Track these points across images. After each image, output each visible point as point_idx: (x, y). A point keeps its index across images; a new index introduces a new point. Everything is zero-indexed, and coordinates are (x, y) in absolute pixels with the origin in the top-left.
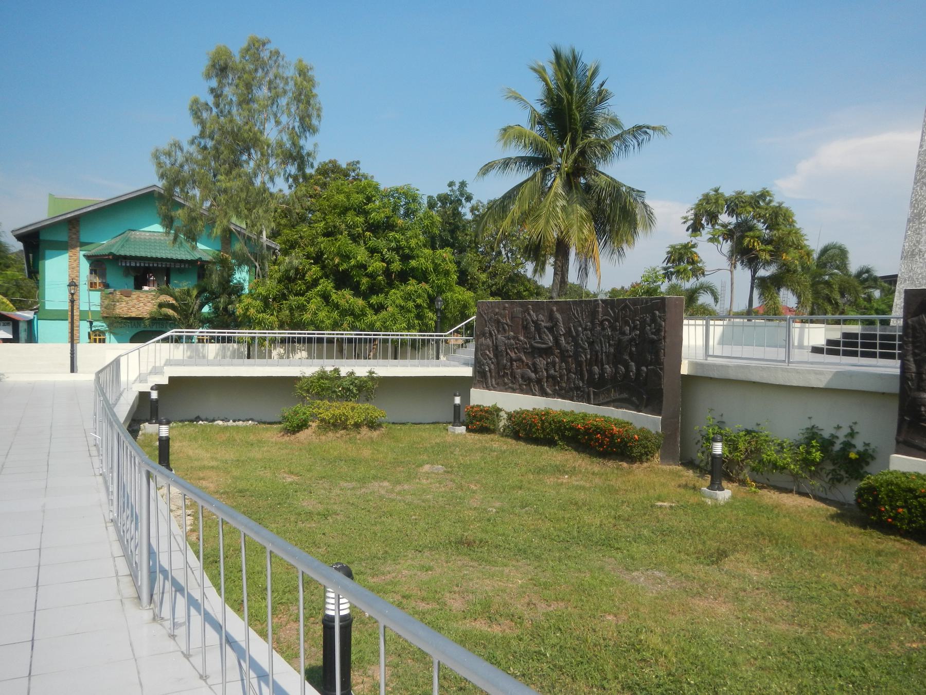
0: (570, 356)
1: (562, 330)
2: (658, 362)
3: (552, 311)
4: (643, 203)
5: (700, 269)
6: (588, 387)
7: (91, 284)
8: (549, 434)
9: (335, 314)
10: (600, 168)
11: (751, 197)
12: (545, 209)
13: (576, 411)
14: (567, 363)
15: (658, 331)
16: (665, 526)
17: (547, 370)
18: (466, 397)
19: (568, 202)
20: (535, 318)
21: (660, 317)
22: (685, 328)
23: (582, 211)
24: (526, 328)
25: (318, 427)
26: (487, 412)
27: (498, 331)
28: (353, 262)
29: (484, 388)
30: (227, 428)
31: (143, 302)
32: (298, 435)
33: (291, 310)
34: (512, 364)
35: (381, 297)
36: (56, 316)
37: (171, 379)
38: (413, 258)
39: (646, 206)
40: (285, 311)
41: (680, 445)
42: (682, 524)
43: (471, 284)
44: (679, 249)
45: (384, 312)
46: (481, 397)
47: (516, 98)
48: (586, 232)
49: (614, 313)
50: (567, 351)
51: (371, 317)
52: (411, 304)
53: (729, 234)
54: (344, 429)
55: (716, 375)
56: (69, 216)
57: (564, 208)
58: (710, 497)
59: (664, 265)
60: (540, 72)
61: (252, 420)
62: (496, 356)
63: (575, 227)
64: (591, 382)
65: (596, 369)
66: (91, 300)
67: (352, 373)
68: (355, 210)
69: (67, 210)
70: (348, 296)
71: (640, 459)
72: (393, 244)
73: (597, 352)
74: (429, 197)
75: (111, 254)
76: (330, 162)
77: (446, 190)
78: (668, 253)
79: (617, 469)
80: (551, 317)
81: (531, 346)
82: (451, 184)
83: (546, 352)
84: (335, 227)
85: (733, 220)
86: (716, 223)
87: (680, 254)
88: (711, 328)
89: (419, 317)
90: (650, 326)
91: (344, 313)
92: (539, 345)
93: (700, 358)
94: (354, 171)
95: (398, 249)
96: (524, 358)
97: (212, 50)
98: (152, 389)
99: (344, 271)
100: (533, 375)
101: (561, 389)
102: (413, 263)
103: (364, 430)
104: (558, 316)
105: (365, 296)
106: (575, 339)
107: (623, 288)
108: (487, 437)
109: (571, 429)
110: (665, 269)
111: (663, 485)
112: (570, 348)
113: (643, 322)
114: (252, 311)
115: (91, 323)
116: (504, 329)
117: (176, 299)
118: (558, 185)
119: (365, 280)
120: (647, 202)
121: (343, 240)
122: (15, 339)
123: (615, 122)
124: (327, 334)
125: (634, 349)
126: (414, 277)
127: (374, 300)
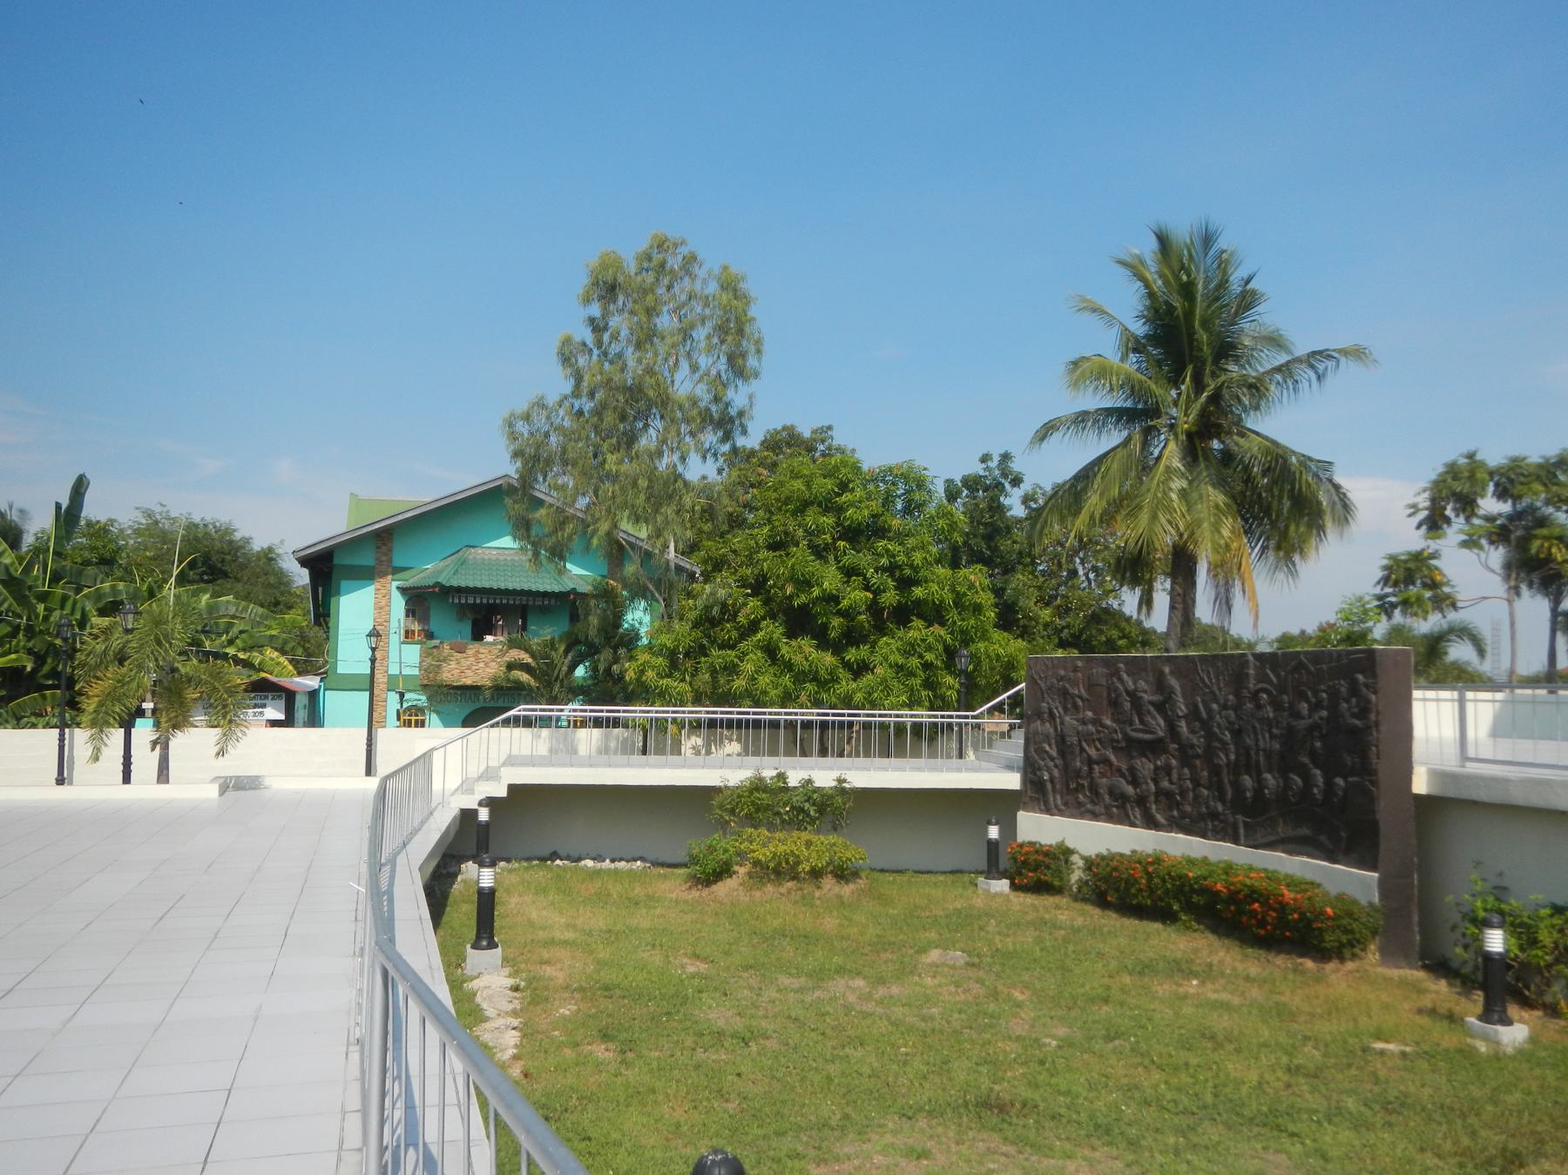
0: (1198, 756)
1: (1182, 709)
2: (1366, 770)
3: (1162, 673)
4: (1330, 481)
5: (1448, 596)
6: (1234, 814)
7: (407, 632)
8: (1161, 899)
9: (787, 680)
10: (1250, 423)
11: (1540, 466)
12: (1150, 496)
13: (1213, 858)
14: (1192, 767)
15: (1364, 710)
16: (1392, 1094)
17: (1155, 781)
18: (1009, 828)
19: (1190, 482)
20: (1131, 686)
21: (1367, 686)
22: (1418, 709)
23: (1218, 497)
24: (1114, 704)
25: (749, 874)
26: (1047, 854)
27: (1066, 709)
28: (816, 592)
29: (1041, 811)
30: (598, 872)
31: (483, 662)
32: (714, 888)
33: (714, 672)
34: (1091, 769)
35: (864, 650)
36: (349, 684)
37: (511, 788)
38: (917, 583)
39: (1337, 487)
40: (703, 675)
41: (1420, 931)
42: (1427, 1091)
43: (1025, 627)
44: (1406, 562)
45: (870, 677)
46: (1038, 828)
47: (1094, 310)
48: (1226, 533)
49: (1278, 676)
50: (1192, 746)
51: (846, 684)
52: (914, 662)
53: (1500, 533)
54: (793, 879)
55: (1482, 795)
56: (377, 526)
57: (1183, 494)
58: (1485, 1038)
59: (1378, 590)
60: (1135, 269)
61: (642, 859)
62: (1062, 753)
63: (1205, 525)
64: (1239, 804)
65: (1247, 781)
66: (406, 658)
67: (810, 781)
68: (820, 505)
69: (376, 517)
70: (808, 649)
71: (1337, 953)
72: (884, 561)
73: (1247, 749)
74: (947, 481)
75: (437, 584)
76: (785, 428)
77: (978, 469)
78: (1386, 568)
79: (1295, 971)
80: (1160, 685)
81: (1125, 735)
82: (985, 459)
83: (1153, 748)
84: (786, 533)
85: (1505, 507)
86: (1473, 514)
87: (1408, 569)
88: (1470, 707)
89: (929, 684)
90: (1347, 701)
91: (801, 677)
92: (1141, 735)
93: (1451, 763)
94: (823, 441)
95: (891, 569)
96: (1113, 758)
97: (594, 261)
98: (480, 804)
99: (804, 608)
100: (1130, 790)
101: (1183, 815)
102: (918, 592)
103: (828, 882)
104: (1174, 683)
105: (837, 648)
106: (1206, 725)
107: (1303, 632)
108: (1050, 900)
109: (1204, 891)
110: (1380, 598)
111: (1386, 1007)
112: (1198, 741)
113: (1334, 695)
114: (650, 674)
115: (402, 695)
116: (1075, 706)
117: (533, 656)
118: (1170, 453)
119: (836, 622)
120: (1338, 479)
121: (800, 553)
122: (288, 722)
123: (1275, 341)
124: (769, 713)
125: (1318, 744)
126: (920, 616)
127: (852, 655)
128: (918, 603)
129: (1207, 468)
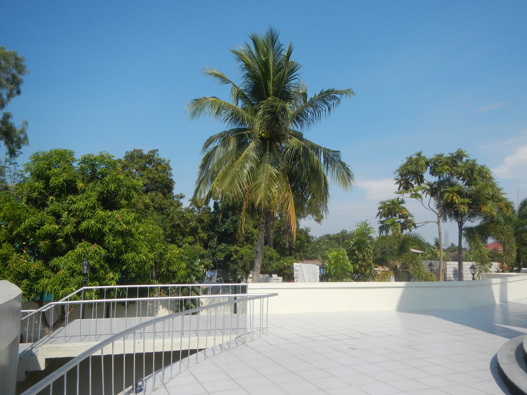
4: (340, 161)
5: (410, 221)
11: (449, 158)
23: (274, 171)
44: (388, 205)
53: (433, 191)
63: (263, 185)
78: (380, 208)
85: (434, 179)
86: (422, 181)
87: (389, 209)
102: (84, 225)
105: (46, 258)
110: (382, 222)
128: (87, 230)
129: (270, 155)
